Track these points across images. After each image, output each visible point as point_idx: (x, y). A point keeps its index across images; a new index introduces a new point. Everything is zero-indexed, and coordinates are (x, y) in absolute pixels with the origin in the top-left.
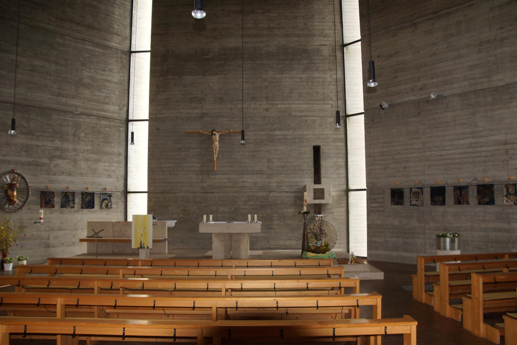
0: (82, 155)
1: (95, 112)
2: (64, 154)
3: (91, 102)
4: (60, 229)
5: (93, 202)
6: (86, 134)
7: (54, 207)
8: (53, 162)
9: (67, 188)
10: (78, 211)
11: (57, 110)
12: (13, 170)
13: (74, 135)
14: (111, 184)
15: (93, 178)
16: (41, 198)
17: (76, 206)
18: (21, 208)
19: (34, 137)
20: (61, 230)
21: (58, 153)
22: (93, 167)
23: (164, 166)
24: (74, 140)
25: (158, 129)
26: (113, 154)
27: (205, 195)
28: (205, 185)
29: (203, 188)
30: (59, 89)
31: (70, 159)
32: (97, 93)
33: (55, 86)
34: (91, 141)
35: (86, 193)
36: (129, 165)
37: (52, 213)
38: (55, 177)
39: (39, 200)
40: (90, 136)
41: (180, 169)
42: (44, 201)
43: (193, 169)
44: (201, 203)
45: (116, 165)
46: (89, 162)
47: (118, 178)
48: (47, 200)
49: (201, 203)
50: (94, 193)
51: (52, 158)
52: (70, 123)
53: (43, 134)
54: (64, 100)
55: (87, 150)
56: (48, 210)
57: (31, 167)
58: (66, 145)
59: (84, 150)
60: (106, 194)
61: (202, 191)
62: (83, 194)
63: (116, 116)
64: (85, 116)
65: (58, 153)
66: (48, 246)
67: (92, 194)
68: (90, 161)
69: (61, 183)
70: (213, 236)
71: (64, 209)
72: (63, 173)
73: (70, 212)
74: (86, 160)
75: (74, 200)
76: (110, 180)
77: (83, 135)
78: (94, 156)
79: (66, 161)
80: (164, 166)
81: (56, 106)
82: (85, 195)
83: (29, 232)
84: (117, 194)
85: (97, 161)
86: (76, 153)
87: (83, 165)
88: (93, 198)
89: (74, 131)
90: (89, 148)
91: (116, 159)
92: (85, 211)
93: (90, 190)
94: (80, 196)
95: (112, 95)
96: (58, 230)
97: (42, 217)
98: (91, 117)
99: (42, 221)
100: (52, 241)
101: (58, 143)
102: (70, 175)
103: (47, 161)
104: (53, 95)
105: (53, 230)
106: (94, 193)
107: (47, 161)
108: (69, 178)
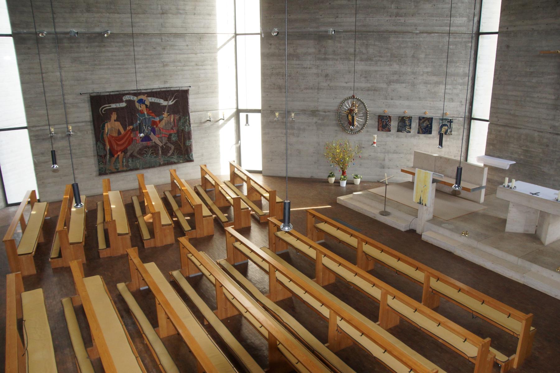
0: (421, 78)
1: (437, 29)
2: (402, 78)
3: (433, 17)
4: (395, 152)
5: (431, 128)
6: (426, 55)
7: (390, 131)
8: (392, 86)
9: (404, 113)
10: (414, 136)
11: (395, 32)
12: (353, 96)
13: (413, 56)
14: (455, 109)
15: (432, 103)
16: (378, 122)
17: (412, 131)
18: (359, 131)
19: (373, 62)
20: (397, 153)
21: (396, 77)
22: (433, 91)
23: (510, 93)
24: (412, 63)
25: (508, 47)
26: (457, 75)
27: (556, 136)
28: (557, 124)
29: (554, 127)
30: (398, 8)
31: (409, 83)
32: (440, 6)
33: (393, 6)
34: (432, 62)
35: (423, 118)
36: (476, 87)
37: (388, 136)
38: (392, 101)
39: (377, 123)
40: (430, 57)
41: (528, 99)
42: (381, 125)
43: (544, 101)
44: (547, 146)
45: (460, 87)
46: (429, 86)
47: (461, 102)
48: (384, 123)
49: (547, 146)
50: (432, 118)
51: (389, 83)
52: (410, 44)
53: (381, 59)
54: (402, 20)
55: (427, 72)
56: (384, 134)
57: (370, 92)
58: (404, 68)
59: (424, 72)
60: (446, 119)
61: (551, 131)
62: (420, 119)
63: (463, 29)
64: (425, 35)
65: (396, 77)
66: (383, 167)
67: (430, 120)
68: (430, 84)
69: (397, 108)
70: (511, 205)
71: (400, 133)
72: (401, 97)
73: (406, 137)
74: (426, 83)
75: (410, 125)
76: (452, 105)
77: (422, 56)
78: (435, 79)
79: (404, 85)
80: (510, 93)
81: (394, 28)
82: (423, 120)
83: (366, 153)
84: (459, 120)
85: (437, 83)
86: (414, 77)
87: (422, 88)
88: (431, 124)
89: (413, 52)
90: (429, 69)
91: (461, 81)
92: (422, 136)
93: (428, 115)
94: (417, 121)
95: (460, 4)
96: (394, 153)
97: (375, 141)
98: (433, 35)
99: (375, 145)
100: (387, 162)
101: (396, 67)
102: (408, 99)
103: (384, 86)
104: (391, 16)
105: (388, 152)
106: (432, 118)
107: (384, 86)
108: (406, 103)
